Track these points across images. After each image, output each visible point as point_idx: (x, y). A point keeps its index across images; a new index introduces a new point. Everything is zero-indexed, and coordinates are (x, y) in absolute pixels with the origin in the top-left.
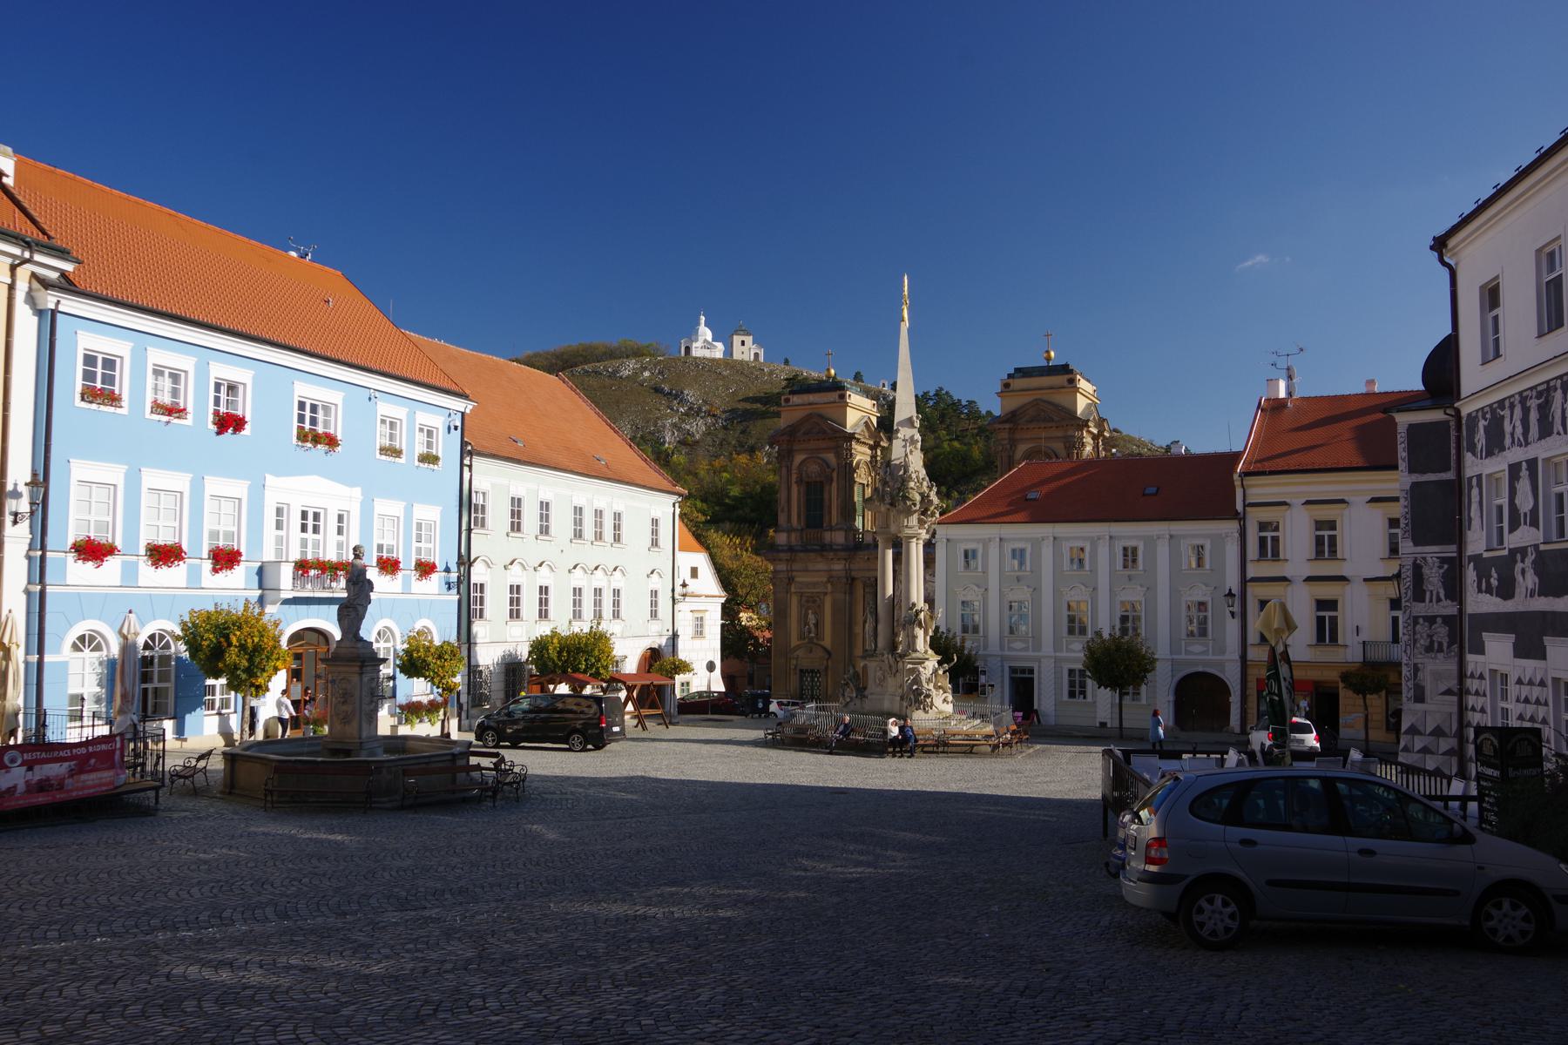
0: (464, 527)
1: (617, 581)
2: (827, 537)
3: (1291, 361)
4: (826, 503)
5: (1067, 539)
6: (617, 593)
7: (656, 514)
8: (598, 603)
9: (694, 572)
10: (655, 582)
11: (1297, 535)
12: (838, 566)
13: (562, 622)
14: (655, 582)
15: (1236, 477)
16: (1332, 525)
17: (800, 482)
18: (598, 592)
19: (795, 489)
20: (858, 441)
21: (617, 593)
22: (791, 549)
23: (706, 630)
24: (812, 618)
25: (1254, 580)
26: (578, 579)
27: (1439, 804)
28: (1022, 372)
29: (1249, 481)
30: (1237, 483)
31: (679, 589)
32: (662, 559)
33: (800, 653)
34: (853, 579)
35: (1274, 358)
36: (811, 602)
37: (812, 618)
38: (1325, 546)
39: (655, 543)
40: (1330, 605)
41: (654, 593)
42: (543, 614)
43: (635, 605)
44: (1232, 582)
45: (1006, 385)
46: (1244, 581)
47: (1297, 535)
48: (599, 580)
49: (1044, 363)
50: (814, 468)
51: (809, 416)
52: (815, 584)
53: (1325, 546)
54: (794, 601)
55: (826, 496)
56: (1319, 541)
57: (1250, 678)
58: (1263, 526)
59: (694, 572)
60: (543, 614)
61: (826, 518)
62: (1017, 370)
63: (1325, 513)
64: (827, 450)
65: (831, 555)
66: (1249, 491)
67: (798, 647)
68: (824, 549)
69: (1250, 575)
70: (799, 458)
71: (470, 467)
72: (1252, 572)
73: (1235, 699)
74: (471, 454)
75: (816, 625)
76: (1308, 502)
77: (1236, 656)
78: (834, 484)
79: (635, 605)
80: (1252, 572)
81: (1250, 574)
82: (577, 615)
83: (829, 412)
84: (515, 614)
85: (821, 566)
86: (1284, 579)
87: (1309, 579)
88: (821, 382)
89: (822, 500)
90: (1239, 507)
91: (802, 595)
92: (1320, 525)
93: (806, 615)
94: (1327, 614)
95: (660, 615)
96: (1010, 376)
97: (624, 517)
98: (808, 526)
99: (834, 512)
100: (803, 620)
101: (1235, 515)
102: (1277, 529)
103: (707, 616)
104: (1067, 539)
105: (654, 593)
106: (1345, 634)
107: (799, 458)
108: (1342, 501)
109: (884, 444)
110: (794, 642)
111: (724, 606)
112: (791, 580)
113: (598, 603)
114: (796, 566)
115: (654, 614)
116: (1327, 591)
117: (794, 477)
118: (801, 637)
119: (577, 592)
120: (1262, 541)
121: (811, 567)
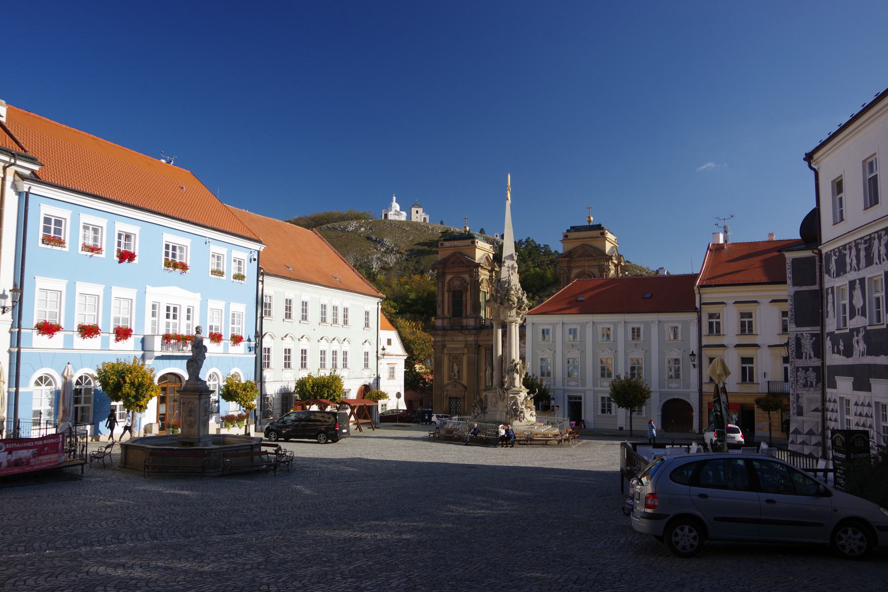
0: (259, 316)
1: (346, 347)
2: (465, 322)
3: (726, 223)
5: (601, 323)
6: (345, 353)
7: (368, 309)
8: (334, 359)
9: (389, 342)
10: (367, 348)
11: (730, 321)
12: (471, 339)
13: (315, 370)
14: (367, 348)
15: (695, 288)
16: (750, 315)
17: (448, 291)
19: (446, 295)
20: (482, 267)
21: (345, 353)
22: (444, 329)
23: (396, 375)
25: (706, 346)
26: (323, 345)
27: (811, 474)
28: (575, 229)
29: (703, 290)
30: (696, 291)
31: (380, 351)
32: (371, 335)
33: (449, 387)
34: (479, 346)
36: (456, 359)
38: (746, 327)
39: (367, 325)
40: (750, 360)
41: (367, 354)
42: (304, 366)
43: (356, 360)
44: (694, 348)
45: (566, 236)
46: (701, 347)
47: (730, 321)
48: (335, 346)
50: (457, 283)
51: (454, 254)
52: (457, 349)
53: (746, 327)
54: (446, 359)
55: (464, 299)
56: (743, 324)
57: (704, 402)
58: (711, 316)
59: (389, 342)
60: (304, 366)
61: (464, 311)
62: (572, 228)
63: (746, 308)
64: (465, 272)
65: (467, 332)
66: (703, 296)
67: (448, 385)
68: (462, 329)
69: (704, 343)
70: (448, 277)
71: (262, 282)
72: (705, 341)
73: (696, 414)
74: (263, 274)
75: (458, 372)
76: (736, 302)
77: (696, 390)
78: (469, 292)
79: (356, 360)
80: (705, 341)
81: (704, 342)
82: (323, 366)
83: (466, 251)
84: (287, 365)
85: (461, 338)
86: (723, 346)
87: (737, 346)
88: (461, 234)
89: (462, 301)
90: (698, 305)
92: (743, 315)
93: (453, 366)
94: (747, 366)
95: (370, 366)
96: (568, 231)
97: (349, 311)
98: (454, 316)
99: (469, 308)
101: (695, 310)
102: (719, 317)
103: (396, 367)
105: (367, 354)
106: (758, 377)
107: (448, 277)
108: (756, 302)
109: (497, 269)
110: (446, 381)
111: (406, 361)
112: (444, 346)
113: (334, 359)
115: (366, 366)
116: (747, 353)
118: (450, 378)
119: (323, 353)
120: (711, 324)
121: (455, 339)
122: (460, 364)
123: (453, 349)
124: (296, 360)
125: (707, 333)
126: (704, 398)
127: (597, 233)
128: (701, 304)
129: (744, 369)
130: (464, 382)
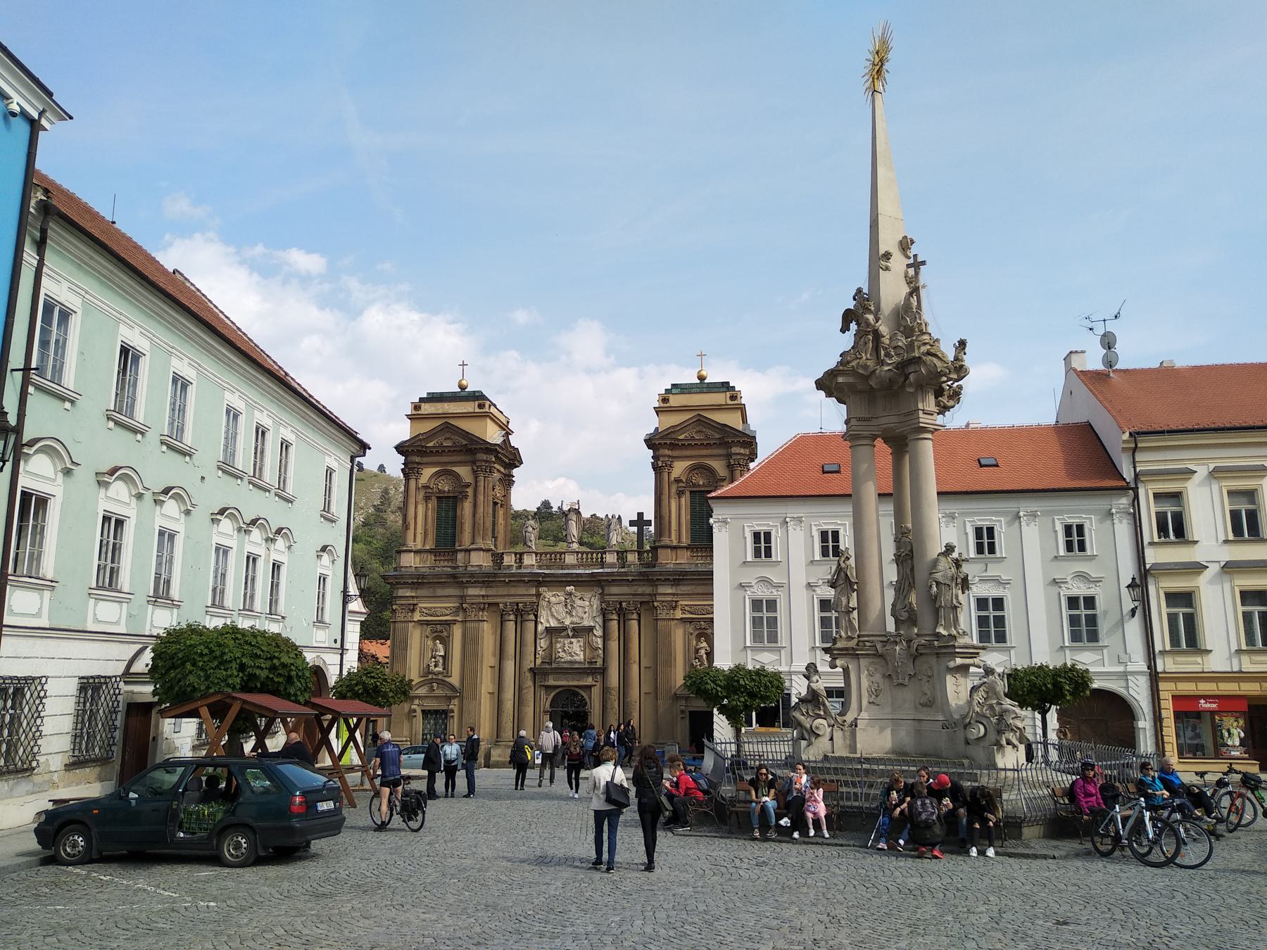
3: (1111, 327)
6: (276, 567)
11: (1206, 510)
12: (472, 591)
17: (427, 498)
18: (252, 560)
21: (276, 567)
44: (1128, 571)
45: (665, 400)
47: (1206, 510)
50: (445, 486)
56: (1235, 516)
62: (673, 385)
72: (1152, 557)
73: (1144, 724)
77: (1143, 667)
82: (218, 601)
84: (108, 580)
91: (428, 623)
101: (1125, 488)
105: (323, 579)
117: (421, 495)
119: (222, 551)
121: (440, 592)
124: (135, 566)
126: (1162, 686)
130: (455, 680)
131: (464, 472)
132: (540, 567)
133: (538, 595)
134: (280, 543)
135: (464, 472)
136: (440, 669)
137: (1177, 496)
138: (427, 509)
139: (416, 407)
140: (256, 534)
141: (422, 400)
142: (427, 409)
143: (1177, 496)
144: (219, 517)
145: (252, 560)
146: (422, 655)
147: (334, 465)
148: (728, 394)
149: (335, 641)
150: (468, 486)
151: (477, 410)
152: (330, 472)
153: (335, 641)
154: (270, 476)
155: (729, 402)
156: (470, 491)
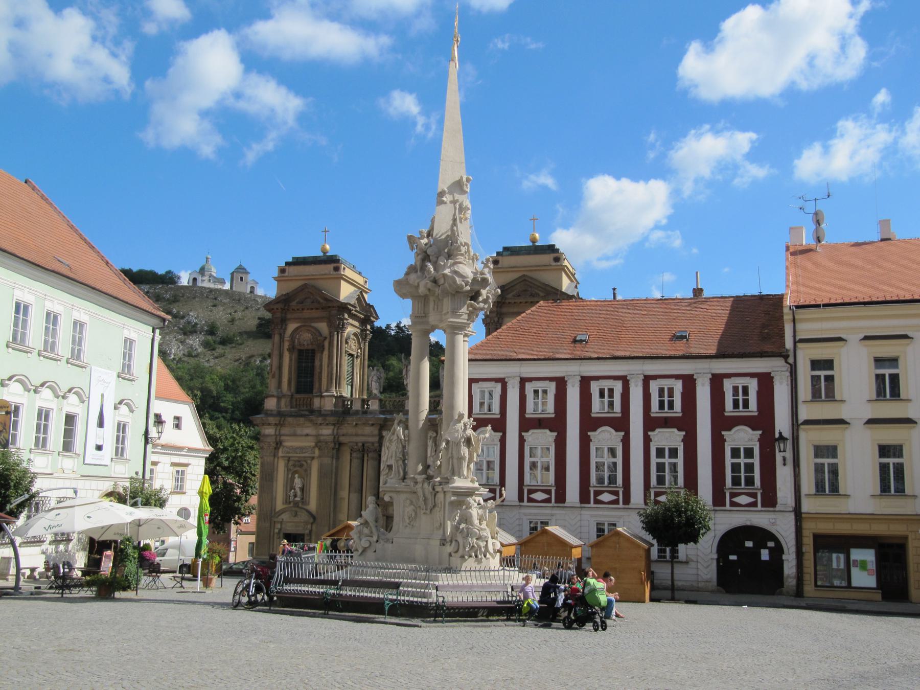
3: (820, 206)
4: (317, 370)
5: (597, 378)
6: (70, 419)
11: (855, 373)
12: (327, 431)
16: (893, 361)
17: (291, 349)
18: (44, 415)
21: (70, 419)
22: (280, 414)
24: (298, 482)
29: (801, 314)
30: (787, 317)
32: (137, 392)
33: (285, 517)
34: (340, 444)
35: (801, 203)
36: (298, 466)
37: (298, 482)
46: (796, 424)
47: (855, 373)
48: (46, 399)
49: (531, 244)
50: (306, 337)
51: (304, 287)
52: (302, 449)
55: (317, 363)
56: (880, 378)
58: (816, 364)
61: (316, 385)
62: (505, 249)
63: (886, 349)
64: (320, 319)
65: (320, 420)
67: (283, 511)
68: (311, 413)
69: (803, 415)
70: (291, 327)
72: (804, 413)
75: (302, 489)
76: (866, 338)
78: (326, 353)
80: (804, 413)
81: (803, 415)
83: (324, 285)
86: (841, 422)
87: (871, 422)
89: (313, 367)
91: (289, 459)
92: (879, 362)
94: (891, 461)
95: (127, 454)
97: (87, 331)
100: (289, 485)
103: (188, 470)
104: (597, 378)
108: (905, 337)
110: (279, 505)
111: (209, 460)
112: (279, 444)
114: (285, 430)
116: (890, 435)
117: (286, 345)
118: (287, 501)
121: (299, 431)
122: (305, 476)
123: (294, 449)
125: (809, 397)
127: (547, 258)
128: (795, 343)
129: (884, 468)
130: (313, 506)
131: (323, 327)
132: (382, 413)
133: (381, 438)
134: (73, 398)
135: (323, 327)
136: (298, 499)
137: (828, 364)
138: (291, 360)
139: (282, 271)
140: (46, 393)
141: (287, 264)
142: (292, 270)
143: (828, 364)
144: (7, 382)
145: (44, 415)
146: (285, 486)
147: (133, 336)
148: (553, 255)
149: (137, 473)
150: (326, 338)
151: (332, 272)
152: (129, 344)
153: (137, 473)
154: (64, 347)
155: (554, 264)
156: (326, 344)
